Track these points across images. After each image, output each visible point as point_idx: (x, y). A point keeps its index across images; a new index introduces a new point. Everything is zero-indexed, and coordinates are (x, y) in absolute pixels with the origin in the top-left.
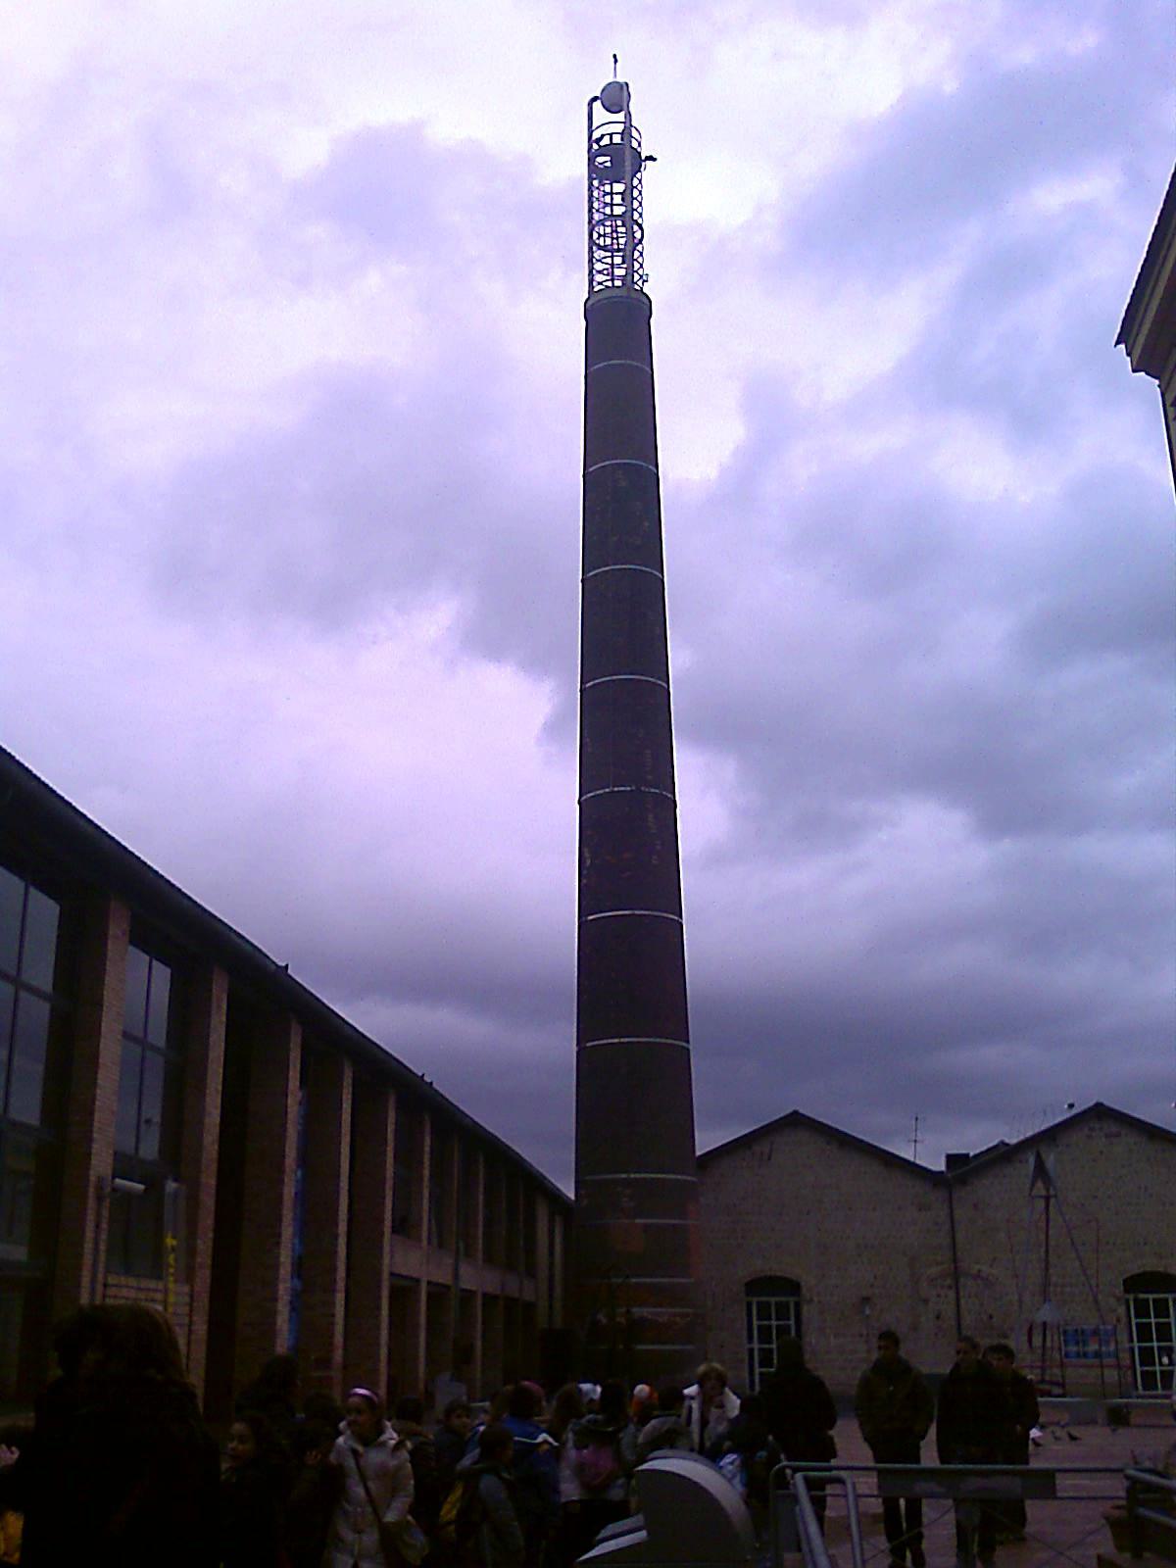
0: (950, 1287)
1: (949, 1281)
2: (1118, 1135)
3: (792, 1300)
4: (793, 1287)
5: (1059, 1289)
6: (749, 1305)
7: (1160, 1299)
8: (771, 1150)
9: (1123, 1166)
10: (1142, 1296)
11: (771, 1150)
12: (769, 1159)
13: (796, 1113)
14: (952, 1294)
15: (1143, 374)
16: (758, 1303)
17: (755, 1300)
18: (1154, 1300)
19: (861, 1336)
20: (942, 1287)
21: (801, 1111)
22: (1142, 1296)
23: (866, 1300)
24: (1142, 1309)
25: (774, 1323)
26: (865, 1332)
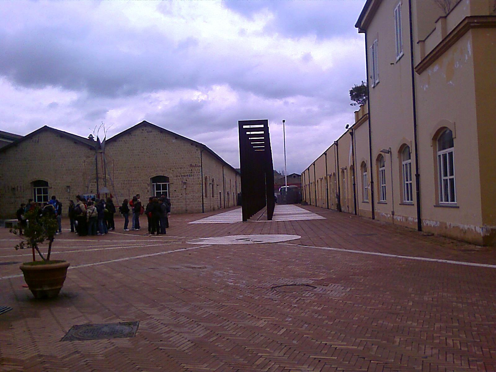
0: (95, 182)
1: (95, 180)
2: (151, 132)
3: (167, 183)
4: (46, 184)
5: (130, 182)
6: (35, 190)
7: (45, 188)
8: (39, 139)
9: (152, 142)
10: (158, 183)
11: (39, 139)
12: (38, 142)
13: (46, 126)
14: (96, 184)
15: (24, 136)
16: (37, 189)
17: (36, 188)
18: (43, 189)
19: (67, 198)
20: (93, 182)
21: (48, 126)
22: (158, 183)
23: (68, 187)
24: (158, 188)
25: (42, 195)
26: (68, 197)
